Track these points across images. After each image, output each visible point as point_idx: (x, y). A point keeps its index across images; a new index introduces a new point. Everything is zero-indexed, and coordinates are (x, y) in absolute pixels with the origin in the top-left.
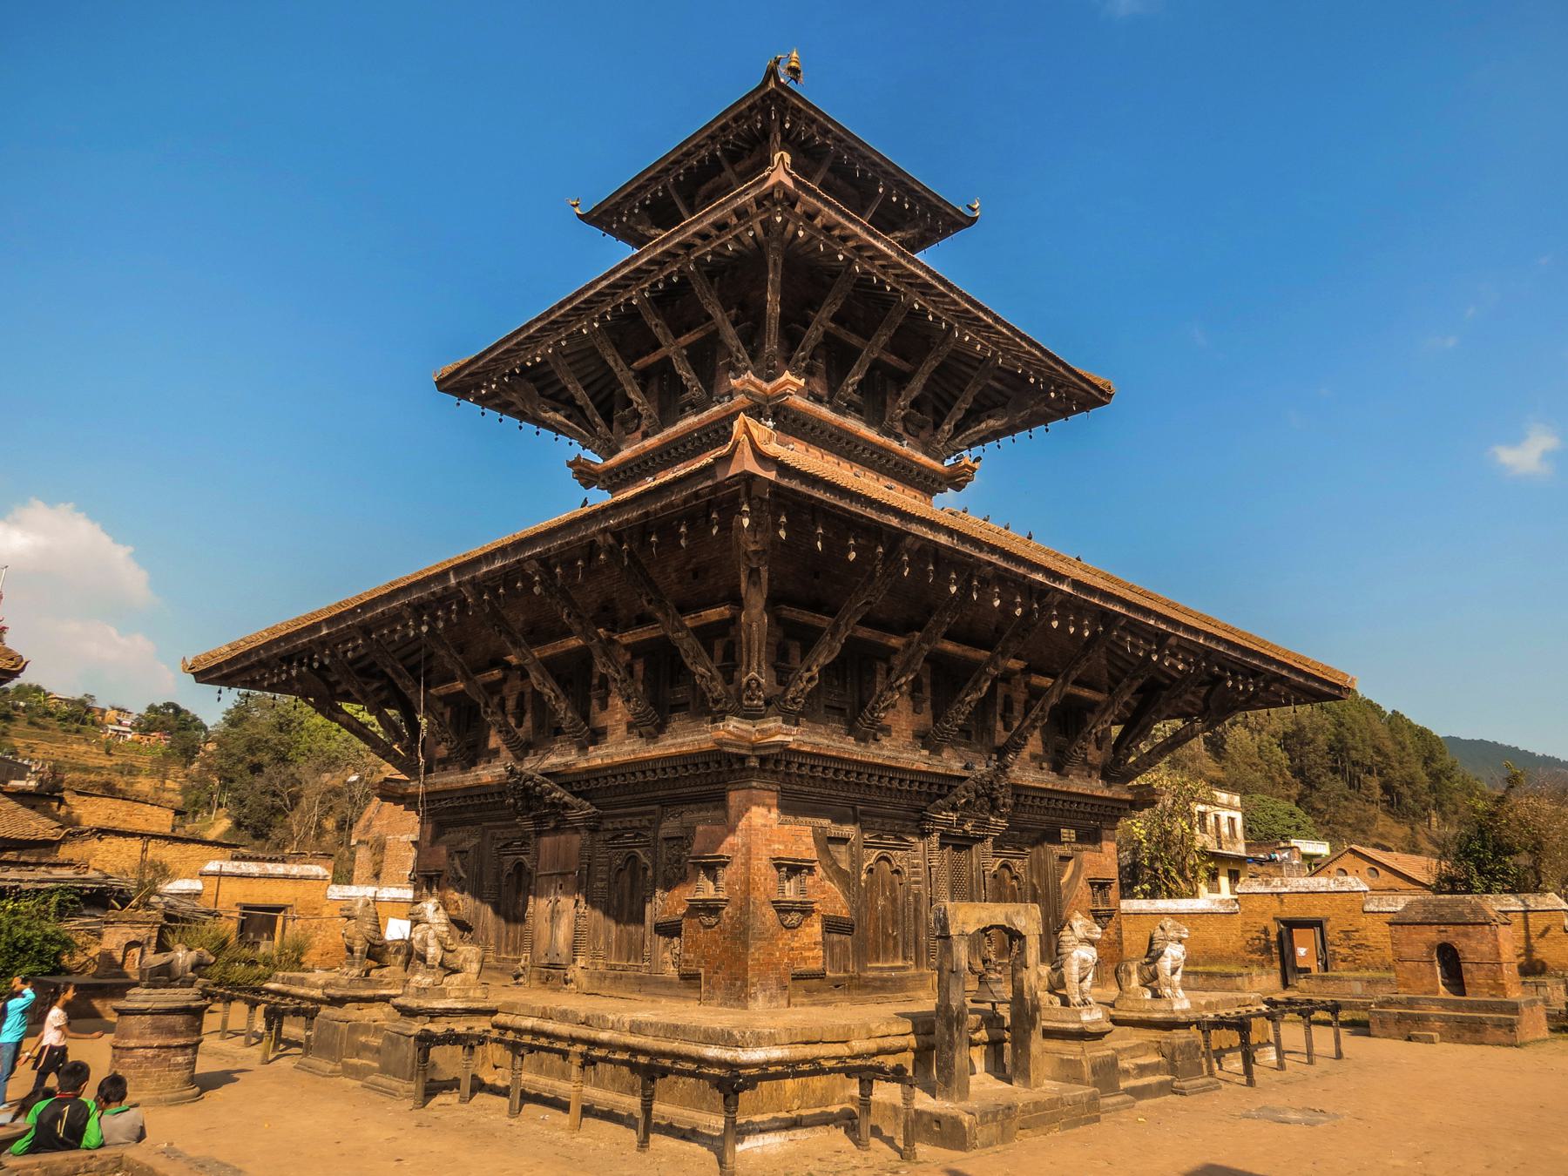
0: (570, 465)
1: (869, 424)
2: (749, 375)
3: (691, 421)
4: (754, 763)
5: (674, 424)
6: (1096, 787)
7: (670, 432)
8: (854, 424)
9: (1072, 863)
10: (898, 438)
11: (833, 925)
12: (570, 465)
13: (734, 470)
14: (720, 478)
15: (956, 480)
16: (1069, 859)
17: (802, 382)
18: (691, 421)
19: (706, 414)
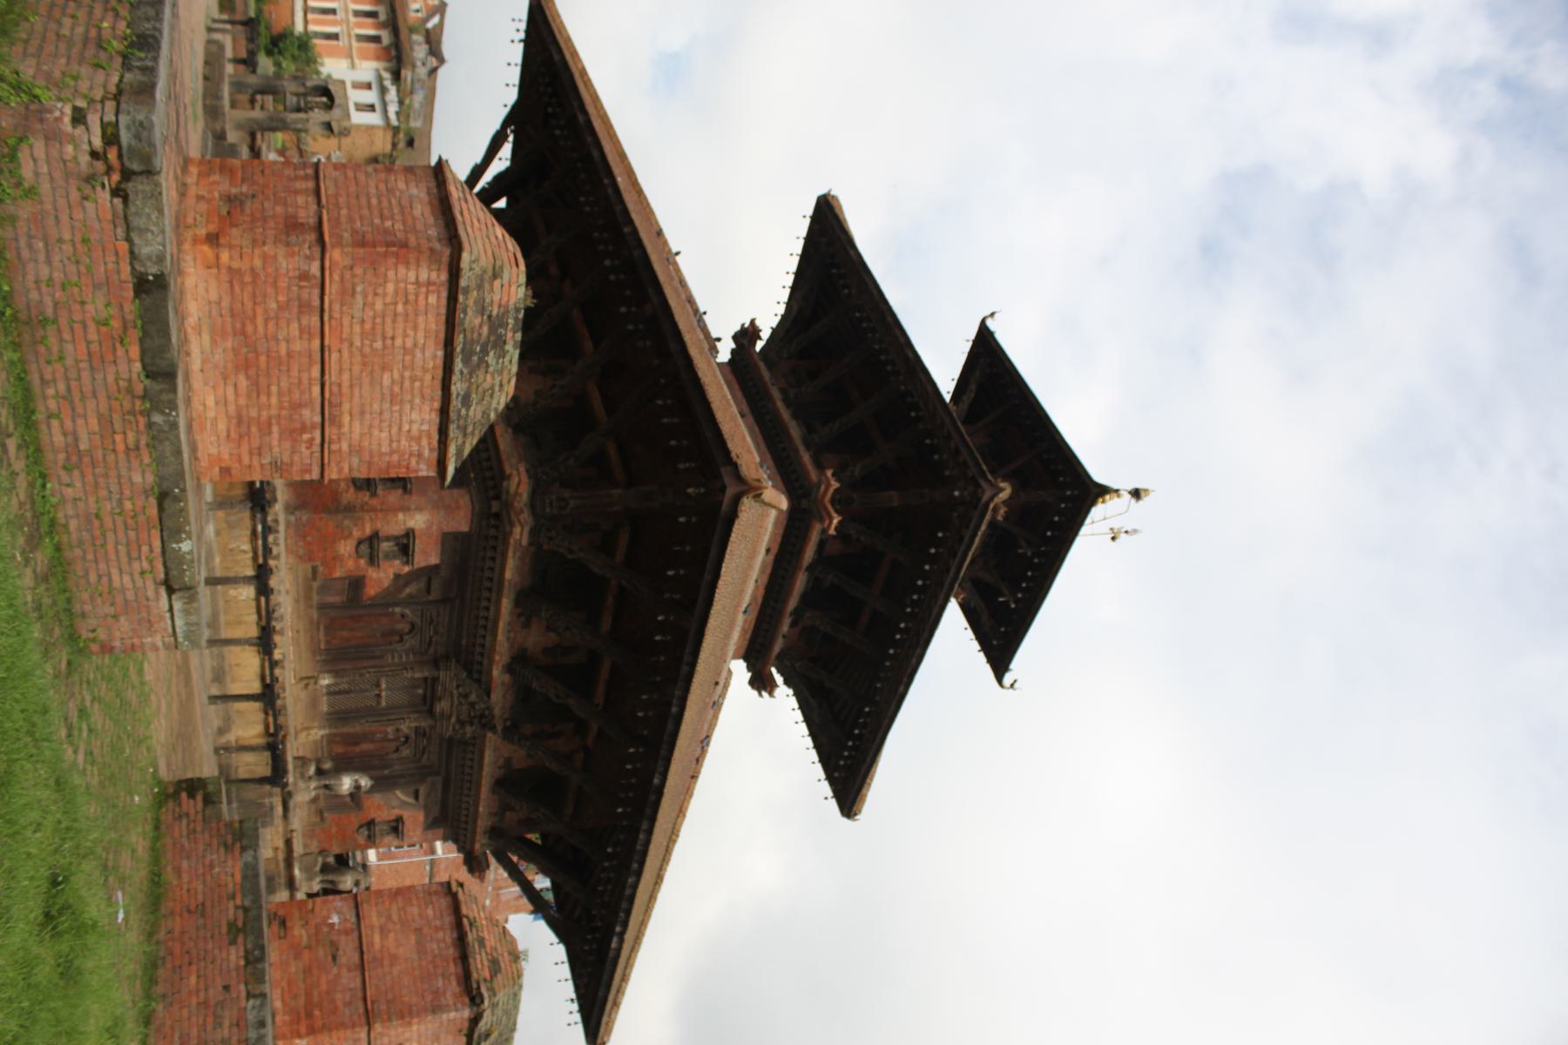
0: (753, 322)
1: (805, 598)
2: (835, 485)
3: (795, 431)
4: (495, 507)
5: (795, 416)
6: (483, 823)
7: (786, 414)
8: (800, 582)
9: (411, 800)
10: (793, 624)
11: (356, 584)
12: (753, 322)
13: (727, 480)
14: (723, 470)
15: (761, 683)
16: (417, 798)
17: (832, 531)
18: (795, 431)
19: (802, 449)
